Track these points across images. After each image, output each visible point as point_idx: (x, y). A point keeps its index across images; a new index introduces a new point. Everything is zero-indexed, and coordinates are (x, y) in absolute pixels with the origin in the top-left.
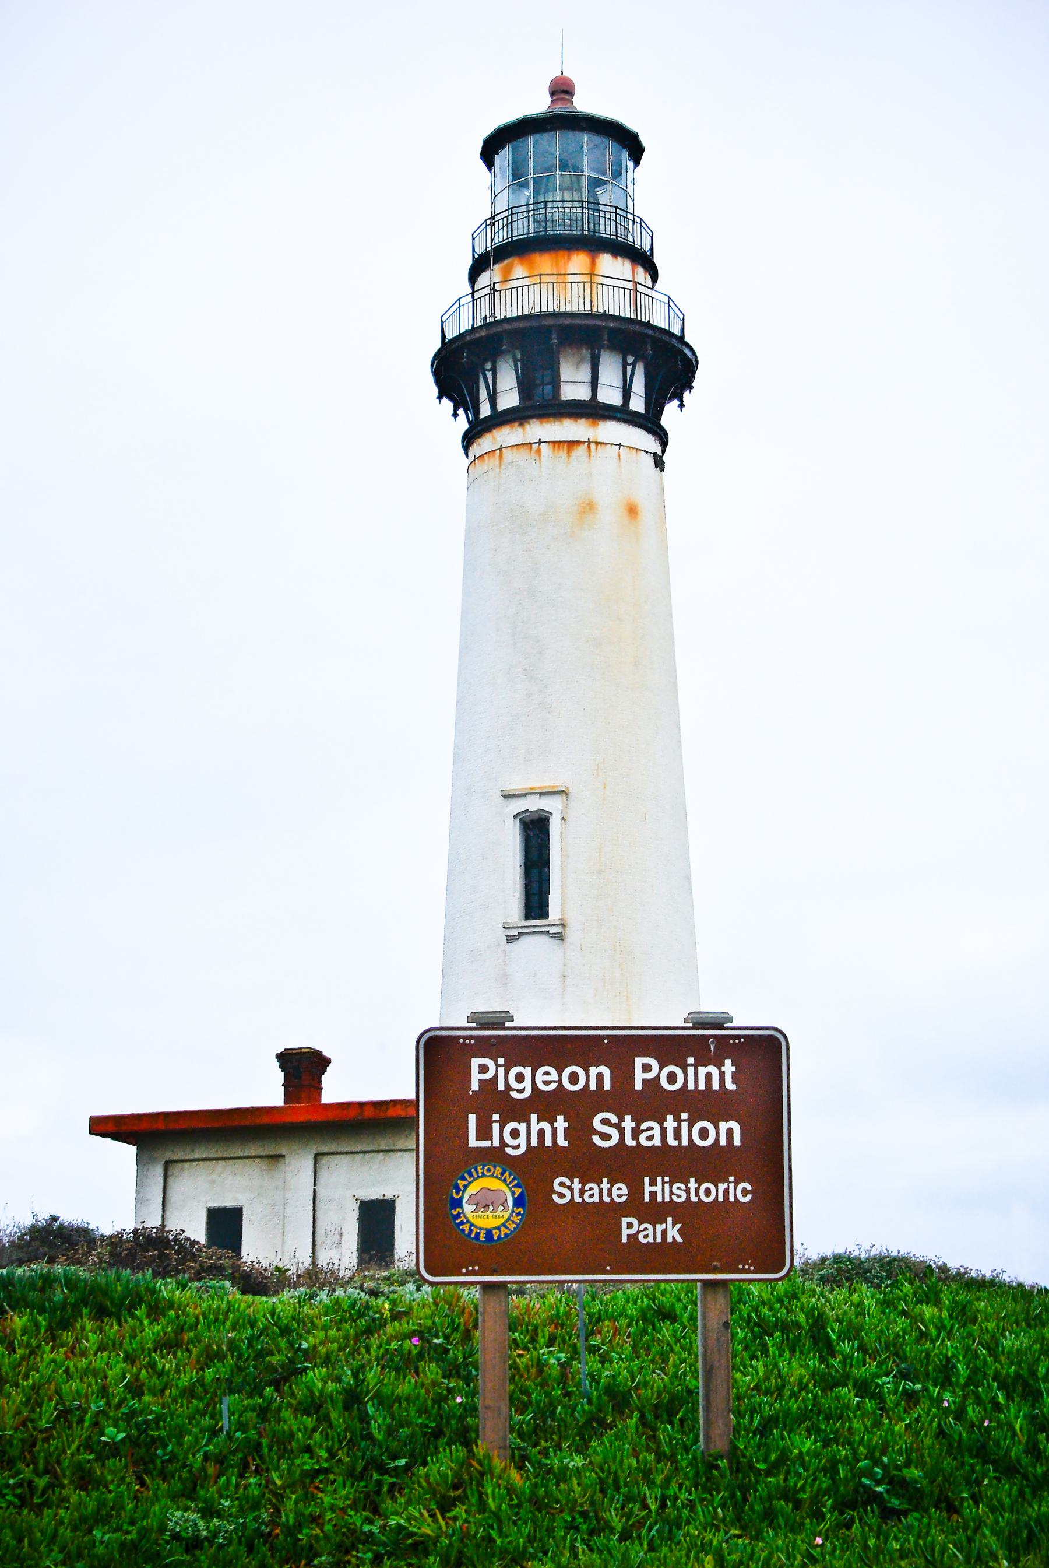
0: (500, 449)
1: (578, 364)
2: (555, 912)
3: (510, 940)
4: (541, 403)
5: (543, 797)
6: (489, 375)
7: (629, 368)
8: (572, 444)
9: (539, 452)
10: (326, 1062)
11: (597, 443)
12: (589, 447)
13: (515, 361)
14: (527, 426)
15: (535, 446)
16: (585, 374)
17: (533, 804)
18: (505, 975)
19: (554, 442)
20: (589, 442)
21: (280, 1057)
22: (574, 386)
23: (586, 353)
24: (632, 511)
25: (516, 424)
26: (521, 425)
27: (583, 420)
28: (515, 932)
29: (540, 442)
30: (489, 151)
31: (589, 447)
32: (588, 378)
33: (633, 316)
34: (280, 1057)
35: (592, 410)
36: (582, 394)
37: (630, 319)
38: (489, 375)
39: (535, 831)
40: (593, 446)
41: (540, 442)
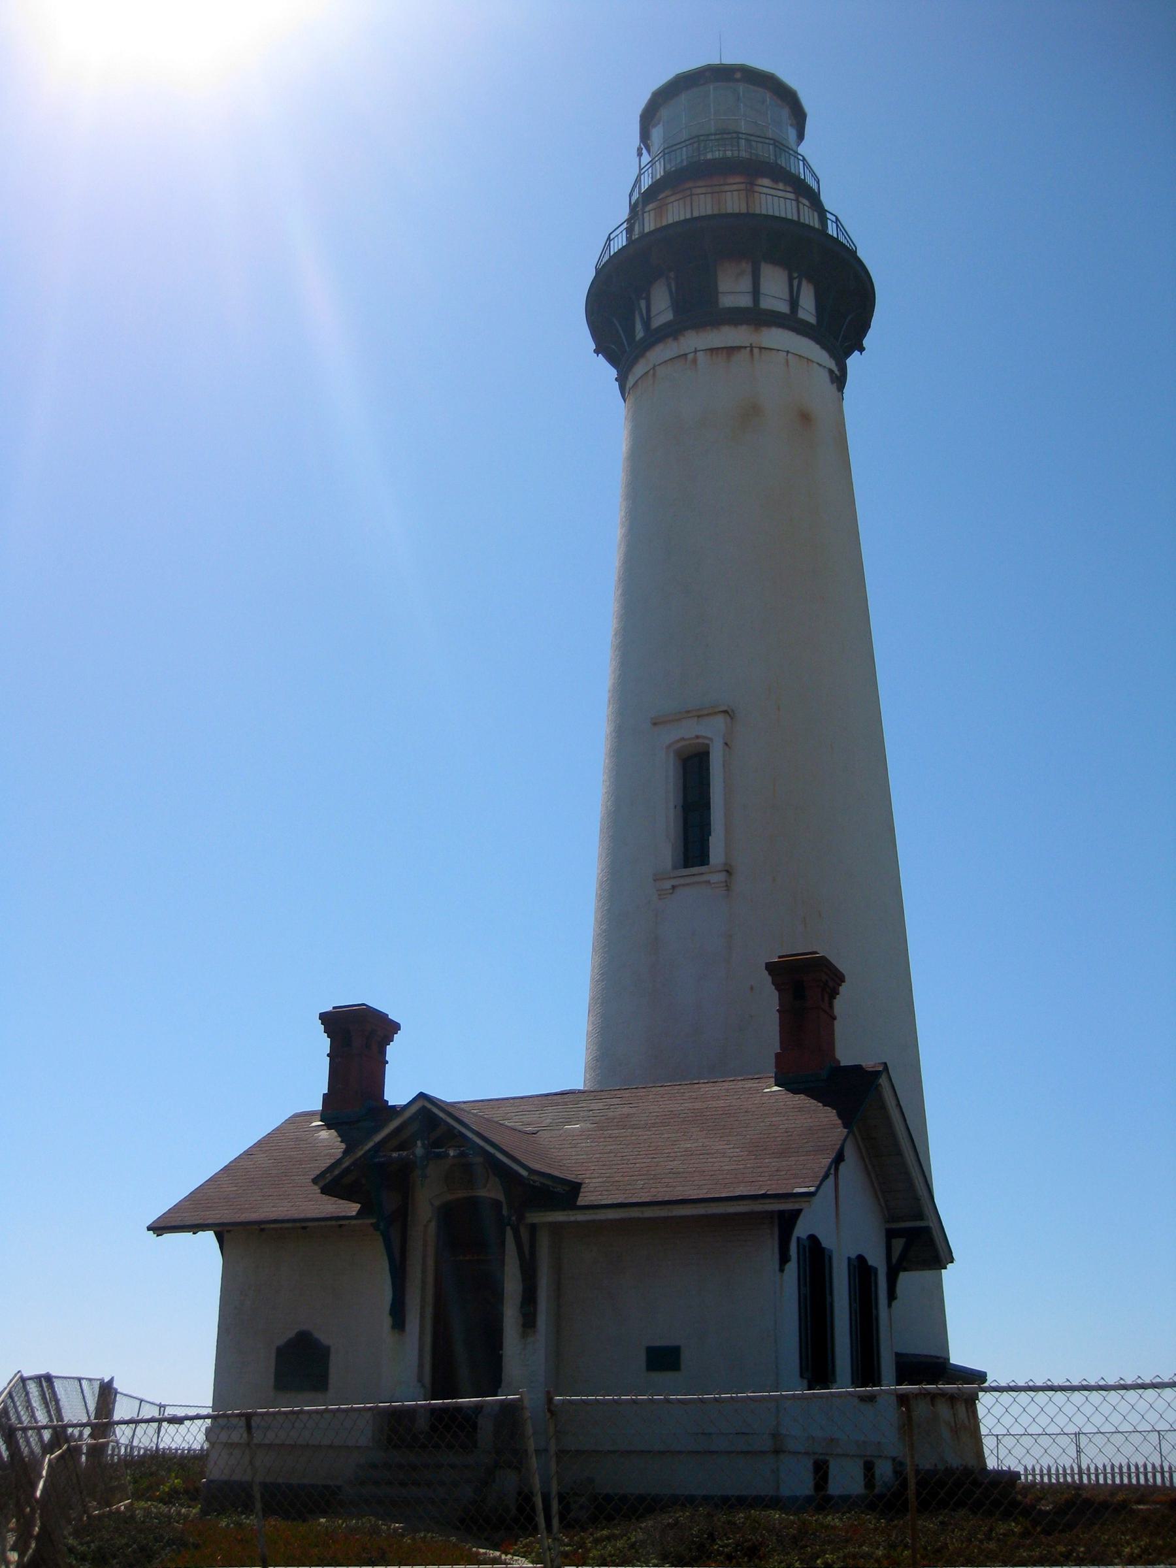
0: (654, 368)
2: (717, 853)
6: (643, 304)
7: (796, 283)
8: (731, 350)
9: (695, 361)
10: (396, 1027)
11: (761, 348)
12: (751, 351)
13: (669, 286)
14: (682, 339)
15: (691, 356)
16: (746, 284)
17: (689, 731)
19: (712, 350)
20: (751, 347)
21: (324, 1017)
22: (733, 290)
23: (746, 267)
24: (805, 418)
25: (670, 340)
26: (676, 339)
27: (744, 327)
28: (668, 884)
31: (751, 351)
33: (795, 218)
34: (324, 1017)
36: (745, 301)
37: (791, 221)
39: (694, 767)
40: (756, 351)
41: (696, 351)
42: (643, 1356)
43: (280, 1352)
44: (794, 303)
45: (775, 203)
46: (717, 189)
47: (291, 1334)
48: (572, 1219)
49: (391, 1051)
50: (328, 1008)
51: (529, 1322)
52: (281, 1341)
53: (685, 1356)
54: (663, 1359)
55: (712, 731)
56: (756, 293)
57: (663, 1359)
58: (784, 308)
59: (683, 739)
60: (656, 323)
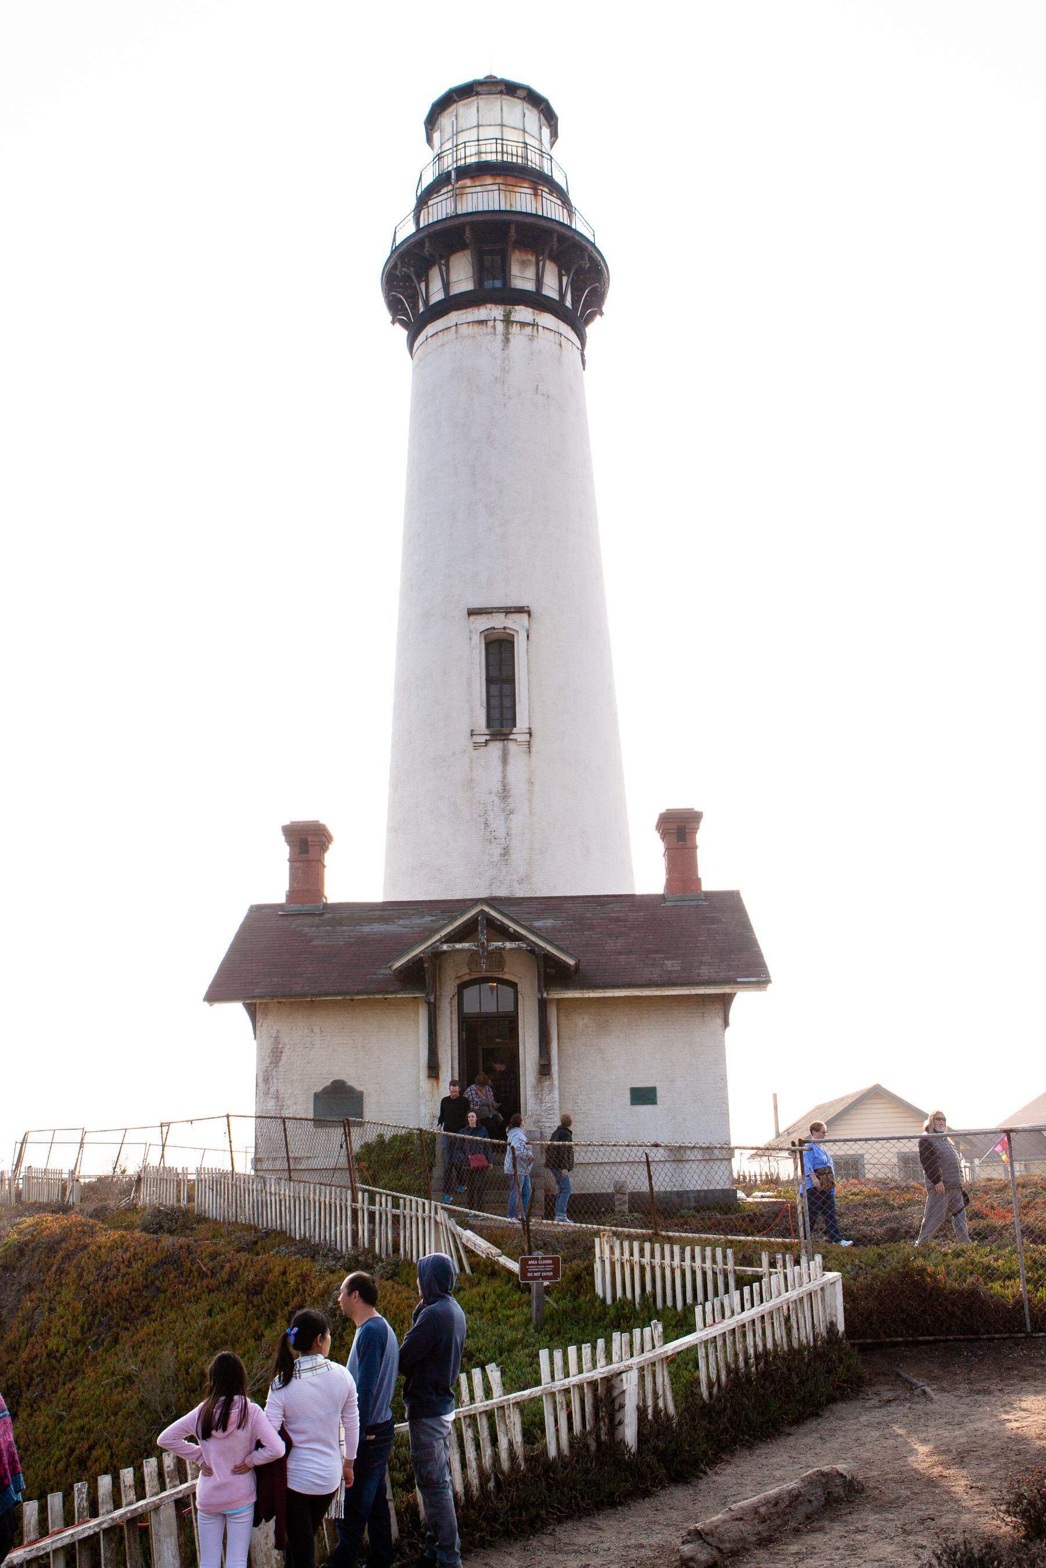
1: (524, 264)
3: (477, 746)
4: (493, 290)
5: (510, 616)
9: (494, 327)
15: (491, 324)
16: (531, 273)
17: (498, 621)
18: (471, 780)
28: (483, 739)
29: (495, 320)
30: (432, 121)
32: (533, 277)
35: (536, 301)
36: (530, 286)
38: (444, 268)
42: (628, 1095)
43: (317, 1096)
44: (562, 296)
45: (553, 210)
46: (510, 188)
47: (328, 1083)
48: (587, 995)
49: (329, 858)
50: (287, 822)
51: (544, 1070)
52: (319, 1089)
53: (660, 1093)
54: (643, 1096)
55: (516, 623)
56: (539, 281)
57: (643, 1096)
58: (555, 296)
59: (494, 628)
60: (457, 289)
